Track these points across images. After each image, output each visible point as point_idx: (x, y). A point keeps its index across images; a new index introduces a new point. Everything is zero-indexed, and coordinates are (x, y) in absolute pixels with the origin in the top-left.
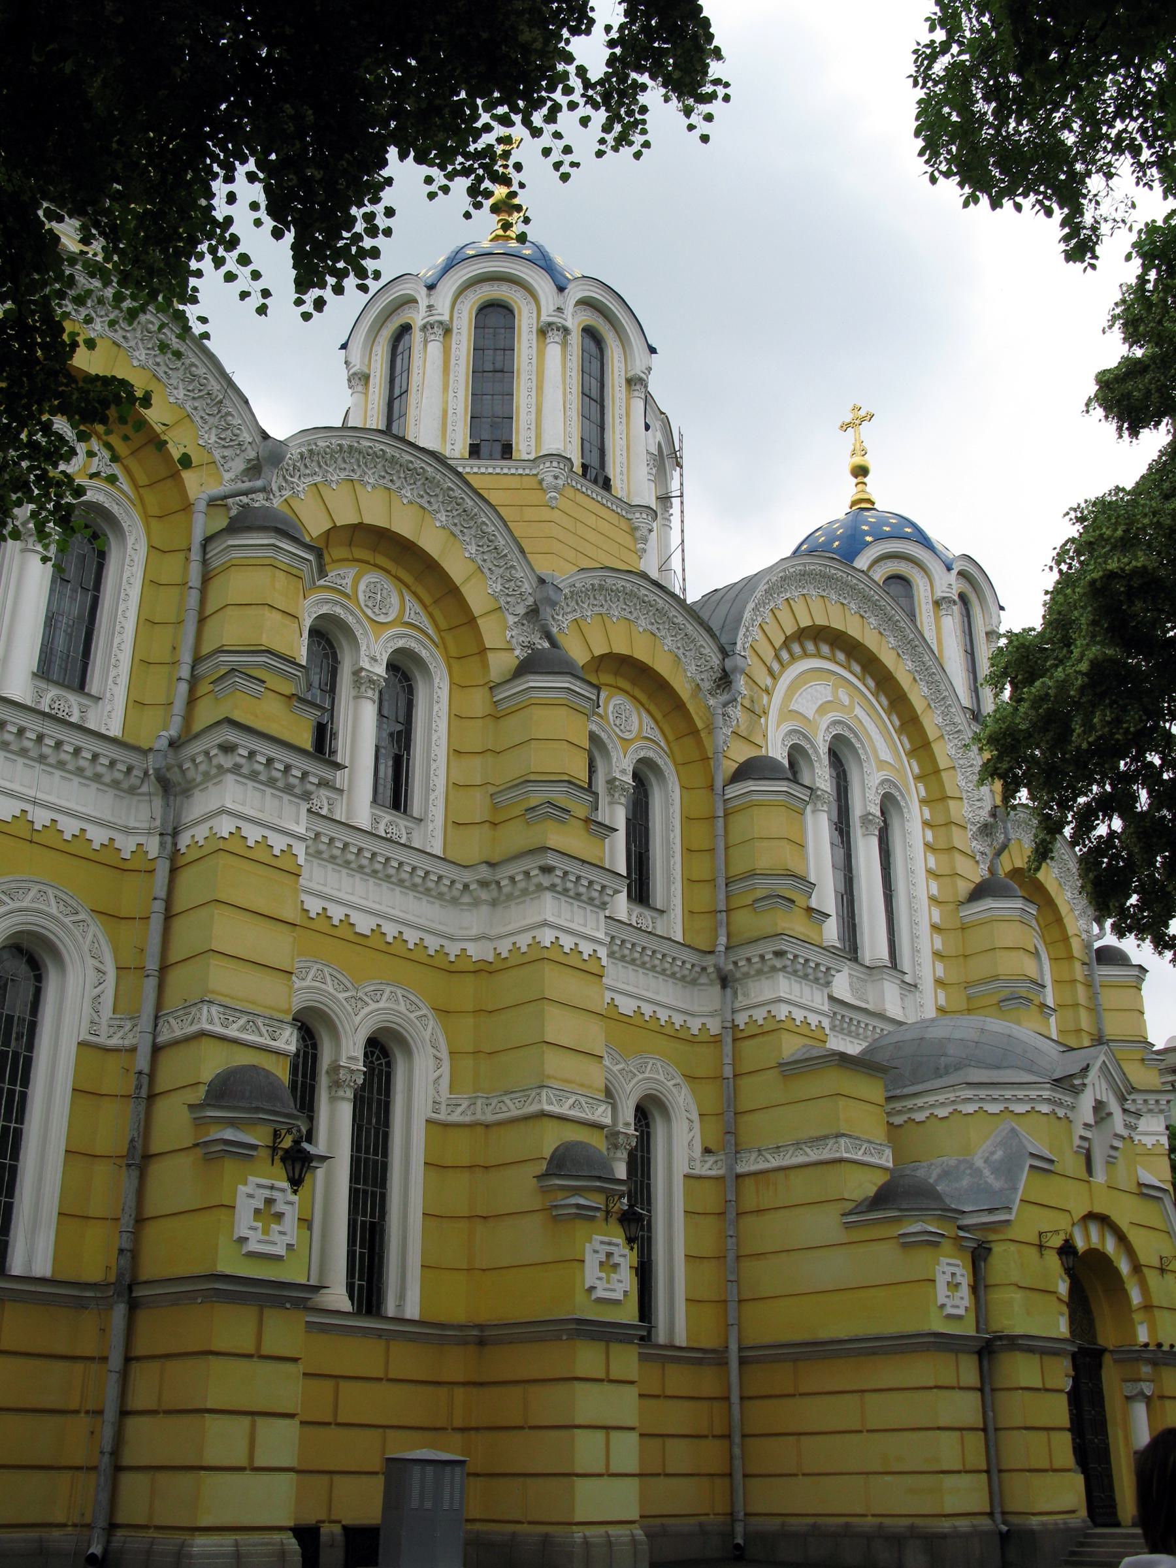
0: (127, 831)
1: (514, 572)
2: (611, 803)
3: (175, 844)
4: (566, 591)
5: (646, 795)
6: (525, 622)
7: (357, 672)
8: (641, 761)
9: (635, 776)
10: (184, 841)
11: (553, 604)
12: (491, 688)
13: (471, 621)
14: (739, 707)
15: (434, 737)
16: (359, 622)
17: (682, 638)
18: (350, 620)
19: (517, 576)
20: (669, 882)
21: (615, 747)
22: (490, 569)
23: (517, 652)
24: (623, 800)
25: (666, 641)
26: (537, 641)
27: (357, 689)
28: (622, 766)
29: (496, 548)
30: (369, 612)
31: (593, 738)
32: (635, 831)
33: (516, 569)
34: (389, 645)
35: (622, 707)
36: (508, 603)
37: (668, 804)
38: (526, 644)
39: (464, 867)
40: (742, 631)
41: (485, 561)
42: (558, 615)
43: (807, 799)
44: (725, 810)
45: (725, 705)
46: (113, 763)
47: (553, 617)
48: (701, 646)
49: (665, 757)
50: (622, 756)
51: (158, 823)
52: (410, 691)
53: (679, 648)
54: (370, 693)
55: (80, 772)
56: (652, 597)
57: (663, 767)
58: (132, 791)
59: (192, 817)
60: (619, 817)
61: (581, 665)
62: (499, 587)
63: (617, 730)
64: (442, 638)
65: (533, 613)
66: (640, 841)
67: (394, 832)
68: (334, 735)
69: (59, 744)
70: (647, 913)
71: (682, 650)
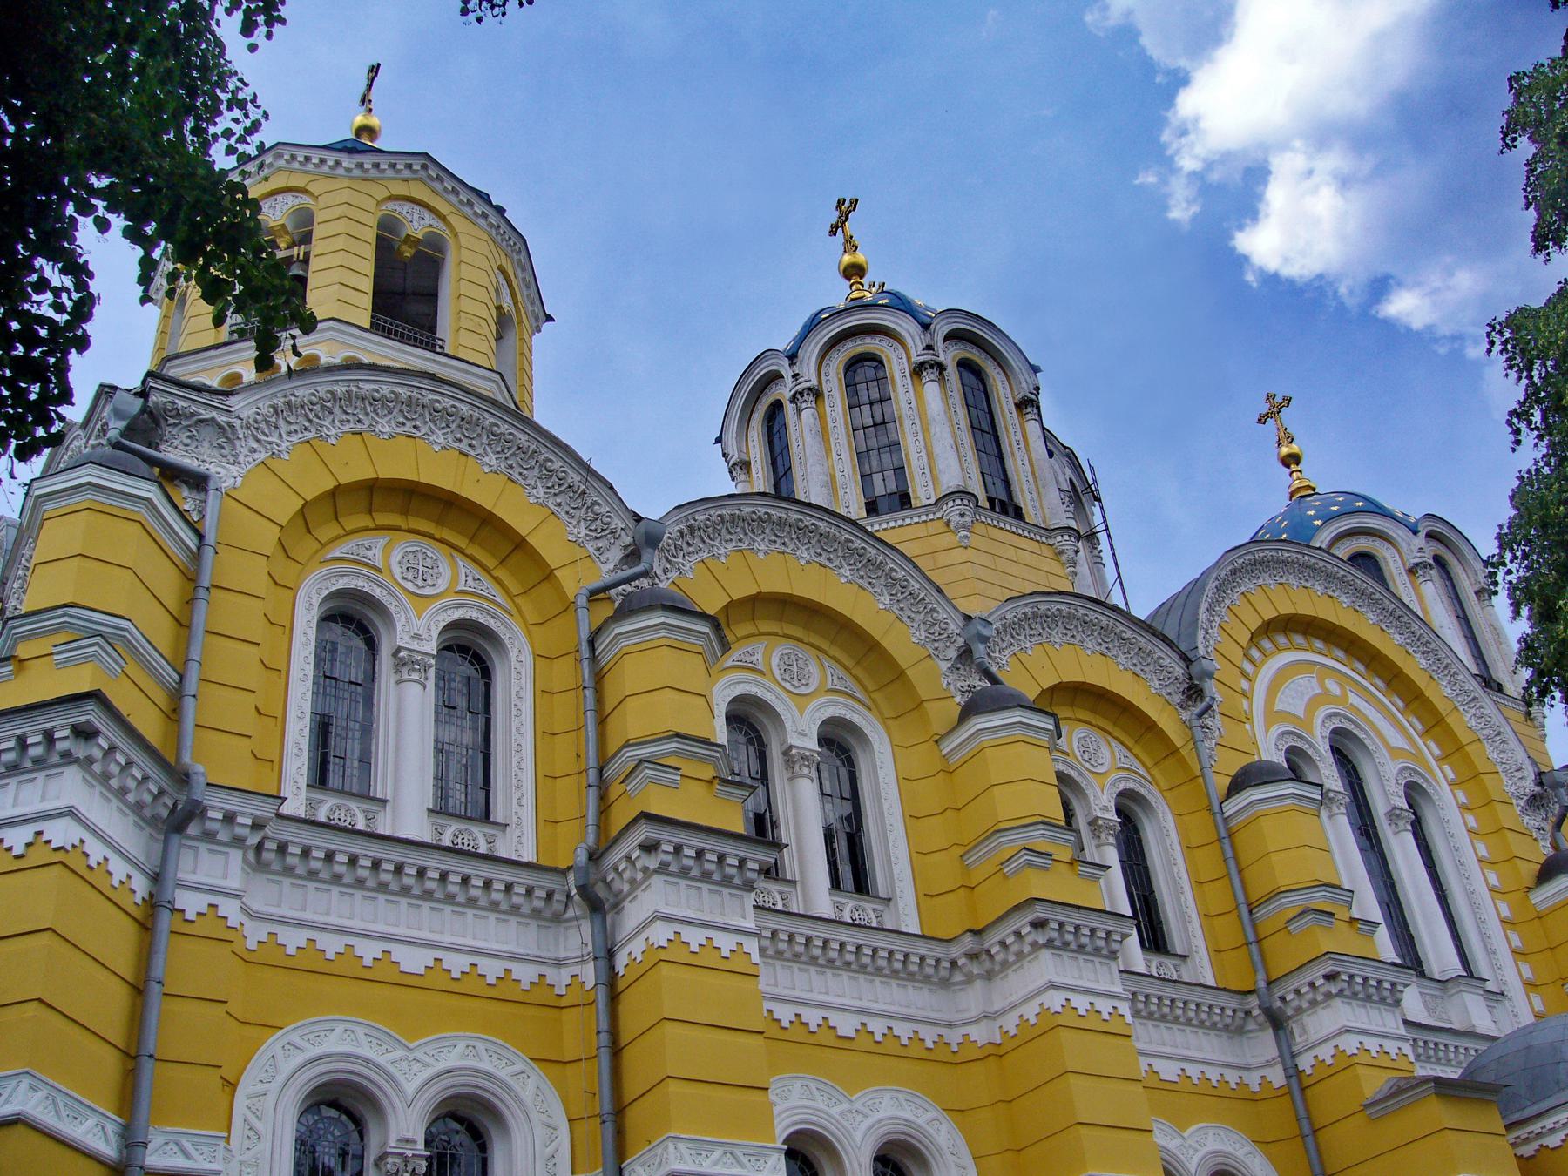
0: (558, 963)
1: (935, 615)
2: (1098, 846)
3: (612, 967)
4: (998, 624)
5: (1137, 831)
6: (959, 666)
7: (786, 752)
8: (1121, 794)
9: (1119, 812)
10: (621, 961)
11: (984, 640)
12: (936, 742)
13: (900, 675)
14: (1218, 716)
15: (886, 806)
16: (390, 592)
17: (1137, 654)
18: (377, 592)
19: (940, 618)
20: (1185, 921)
21: (1089, 783)
22: (909, 617)
23: (958, 699)
24: (1112, 840)
25: (1119, 660)
26: (977, 683)
27: (791, 770)
28: (1101, 802)
29: (911, 594)
30: (787, 686)
31: (1062, 778)
32: (1133, 873)
33: (938, 612)
34: (817, 714)
35: (1087, 739)
36: (936, 649)
37: (1162, 834)
38: (966, 688)
39: (948, 941)
40: (1201, 634)
41: (902, 609)
42: (994, 652)
43: (1320, 798)
44: (1228, 829)
45: (1200, 715)
46: (530, 892)
47: (988, 655)
48: (1160, 658)
49: (1148, 785)
50: (1099, 792)
51: (590, 948)
52: (850, 764)
53: (1135, 665)
54: (805, 771)
55: (494, 906)
56: (1092, 615)
57: (1149, 797)
58: (557, 919)
59: (626, 934)
60: (1112, 856)
61: (1032, 700)
62: (924, 634)
63: (1087, 765)
64: (873, 700)
65: (966, 654)
66: (1141, 880)
67: (861, 918)
68: (775, 825)
69: (466, 880)
70: (1168, 961)
71: (1139, 667)
